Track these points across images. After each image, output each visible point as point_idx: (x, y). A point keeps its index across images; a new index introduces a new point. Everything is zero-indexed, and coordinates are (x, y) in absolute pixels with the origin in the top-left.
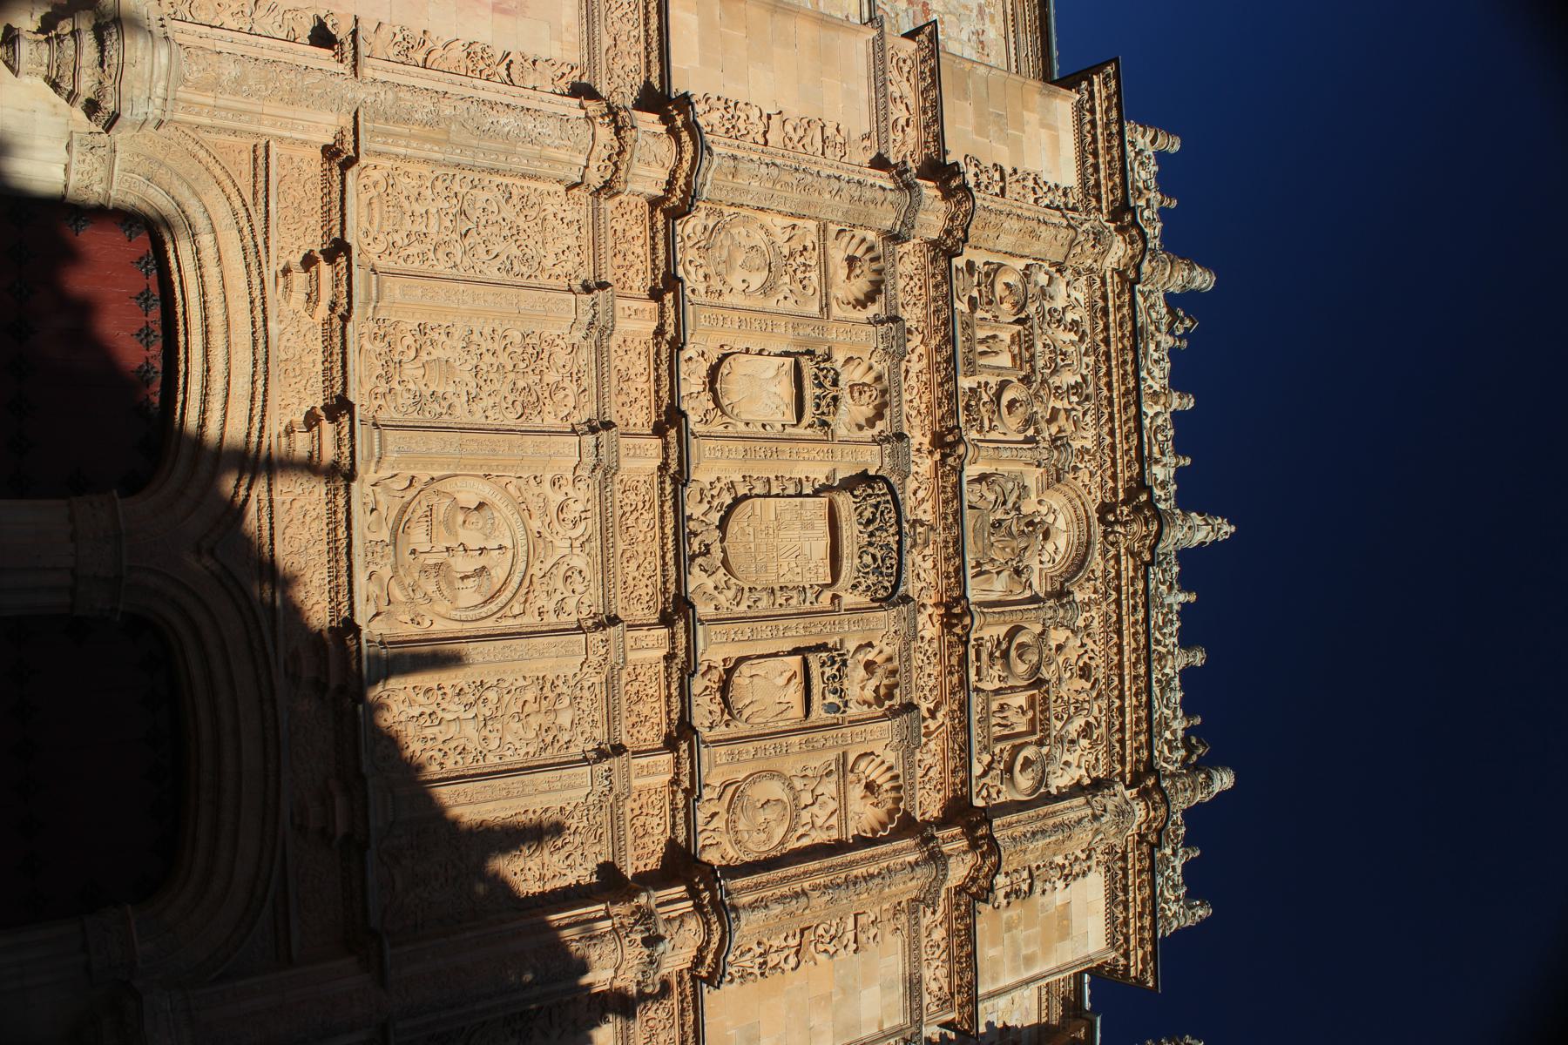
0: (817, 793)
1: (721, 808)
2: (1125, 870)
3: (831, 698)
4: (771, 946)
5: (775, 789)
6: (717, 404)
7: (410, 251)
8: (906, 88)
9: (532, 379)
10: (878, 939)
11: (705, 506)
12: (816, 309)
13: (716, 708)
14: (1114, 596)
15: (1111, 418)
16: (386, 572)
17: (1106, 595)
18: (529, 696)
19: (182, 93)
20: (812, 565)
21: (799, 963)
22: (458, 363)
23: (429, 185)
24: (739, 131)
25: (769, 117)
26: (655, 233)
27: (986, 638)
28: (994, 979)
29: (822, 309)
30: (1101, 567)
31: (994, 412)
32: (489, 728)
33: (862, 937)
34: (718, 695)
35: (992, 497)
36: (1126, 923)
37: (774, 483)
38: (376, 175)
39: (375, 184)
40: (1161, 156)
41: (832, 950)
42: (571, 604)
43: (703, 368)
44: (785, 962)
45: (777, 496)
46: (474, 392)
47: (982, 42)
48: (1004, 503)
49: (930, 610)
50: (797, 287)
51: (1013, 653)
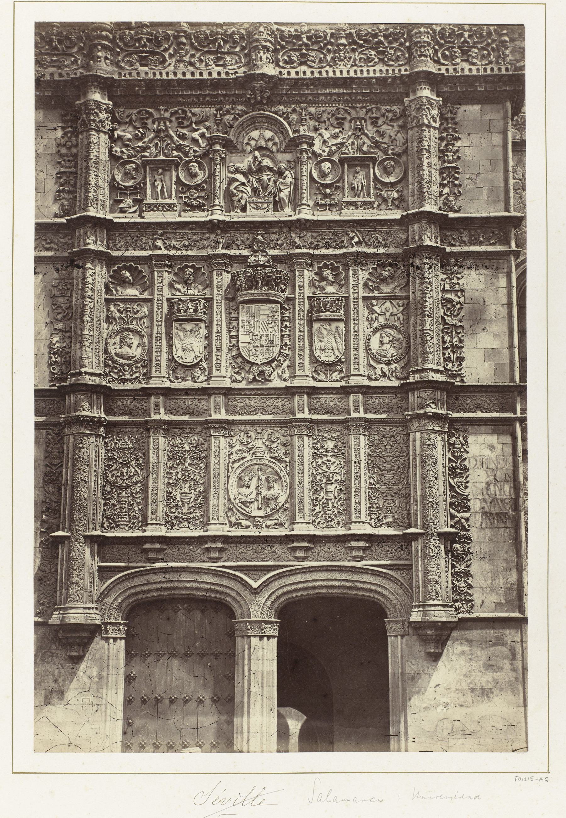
1: (379, 366)
7: (137, 509)
9: (187, 457)
10: (459, 276)
17: (298, 103)
18: (320, 461)
20: (271, 315)
24: (65, 347)
25: (55, 329)
30: (281, 107)
33: (457, 287)
39: (110, 523)
42: (283, 439)
45: (238, 331)
48: (243, 184)
50: (138, 315)
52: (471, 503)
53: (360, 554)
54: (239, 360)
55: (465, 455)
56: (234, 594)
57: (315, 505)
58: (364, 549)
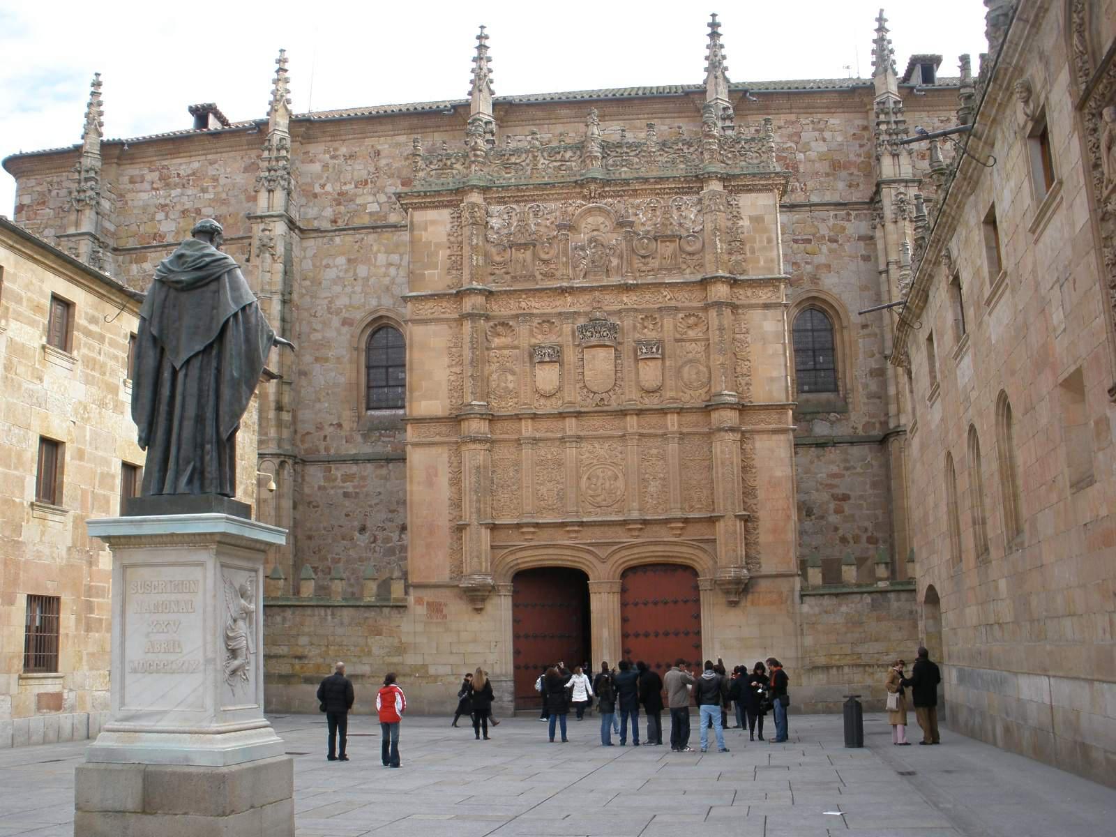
0: (688, 350)
2: (738, 186)
3: (654, 350)
5: (686, 369)
8: (426, 307)
11: (588, 399)
13: (655, 395)
15: (547, 195)
17: (621, 196)
18: (647, 463)
19: (483, 570)
27: (636, 266)
28: (772, 261)
35: (582, 265)
36: (763, 185)
37: (580, 370)
43: (542, 401)
47: (350, 156)
49: (625, 299)
51: (643, 252)
52: (758, 492)
53: (679, 532)
54: (586, 390)
55: (753, 456)
56: (588, 563)
58: (682, 529)
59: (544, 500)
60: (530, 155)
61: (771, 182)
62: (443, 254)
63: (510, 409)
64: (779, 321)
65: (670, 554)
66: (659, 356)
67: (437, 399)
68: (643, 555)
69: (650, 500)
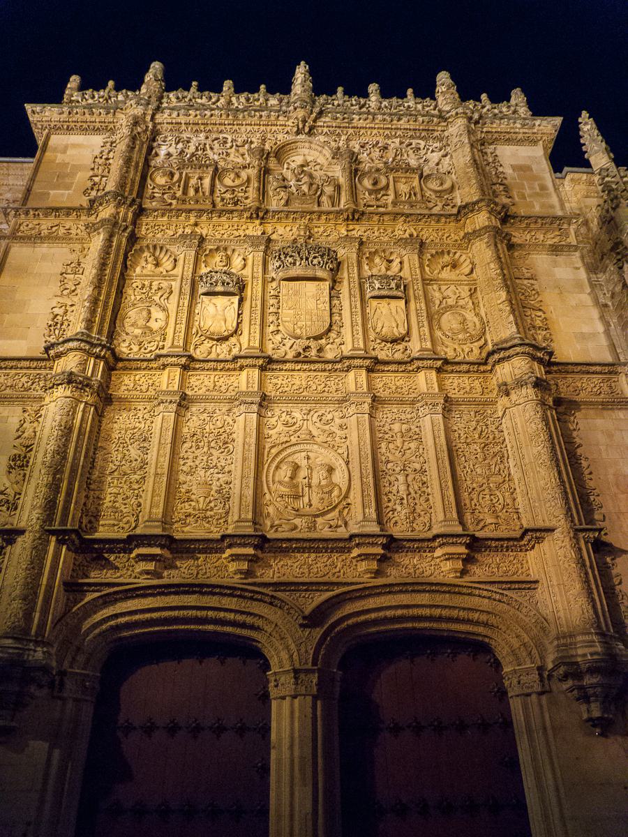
3: (393, 285)
4: (531, 324)
6: (226, 339)
12: (173, 283)
14: (338, 130)
16: (320, 520)
21: (540, 310)
22: (199, 479)
23: (92, 493)
26: (127, 368)
28: (552, 207)
29: (173, 280)
31: (233, 190)
32: (407, 468)
34: (389, 345)
35: (283, 193)
38: (85, 521)
40: (82, 88)
41: (534, 292)
42: (338, 421)
44: (540, 317)
46: (216, 470)
54: (279, 337)
57: (389, 501)
59: (189, 500)
60: (222, 100)
61: (535, 131)
62: (82, 178)
63: (149, 355)
64: (579, 268)
65: (445, 613)
66: (400, 294)
67: (23, 337)
68: (389, 613)
69: (398, 508)
